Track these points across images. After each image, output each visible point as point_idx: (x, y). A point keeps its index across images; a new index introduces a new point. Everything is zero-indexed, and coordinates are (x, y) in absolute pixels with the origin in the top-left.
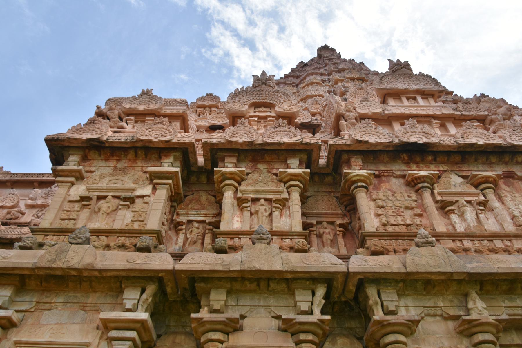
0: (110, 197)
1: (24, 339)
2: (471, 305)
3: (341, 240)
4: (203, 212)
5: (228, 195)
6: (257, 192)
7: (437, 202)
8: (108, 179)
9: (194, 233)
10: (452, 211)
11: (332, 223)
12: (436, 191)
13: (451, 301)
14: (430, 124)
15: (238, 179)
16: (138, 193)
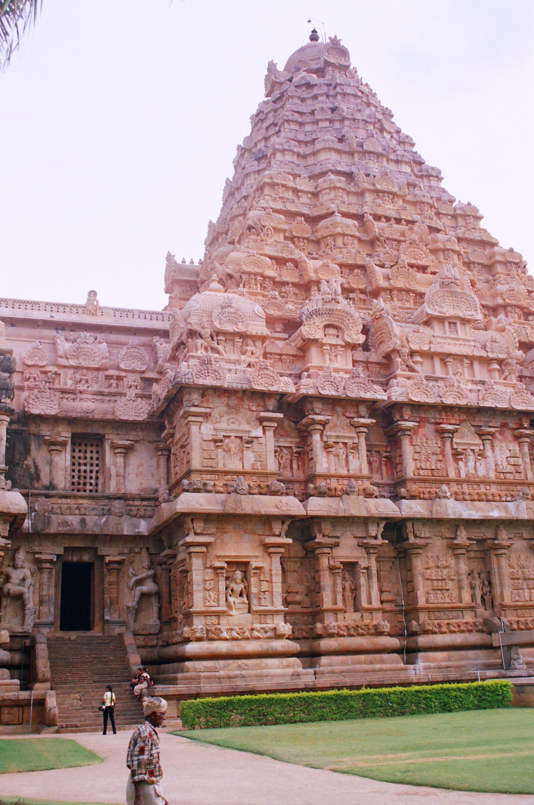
0: (233, 438)
1: (222, 554)
2: (458, 533)
3: (384, 468)
4: (289, 439)
5: (316, 437)
6: (338, 437)
7: (452, 448)
8: (225, 418)
9: (284, 459)
10: (461, 459)
11: (378, 452)
12: (455, 440)
13: (449, 529)
14: (462, 361)
15: (323, 423)
16: (253, 434)
